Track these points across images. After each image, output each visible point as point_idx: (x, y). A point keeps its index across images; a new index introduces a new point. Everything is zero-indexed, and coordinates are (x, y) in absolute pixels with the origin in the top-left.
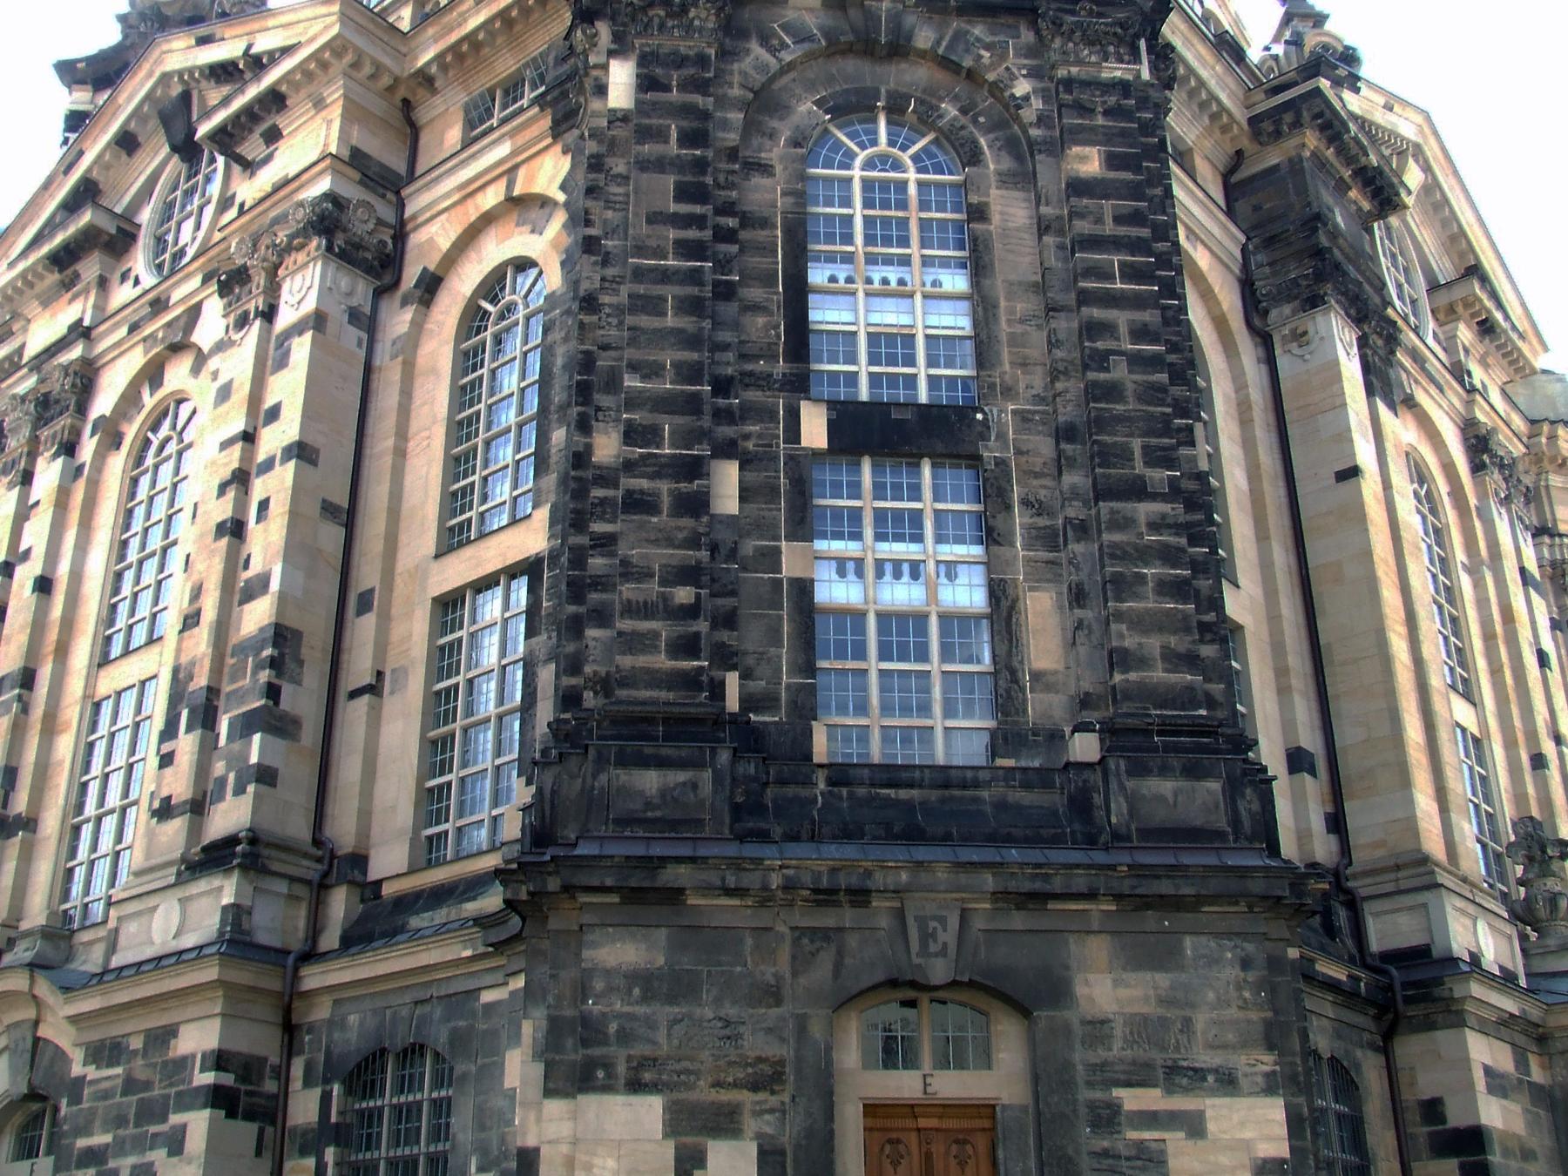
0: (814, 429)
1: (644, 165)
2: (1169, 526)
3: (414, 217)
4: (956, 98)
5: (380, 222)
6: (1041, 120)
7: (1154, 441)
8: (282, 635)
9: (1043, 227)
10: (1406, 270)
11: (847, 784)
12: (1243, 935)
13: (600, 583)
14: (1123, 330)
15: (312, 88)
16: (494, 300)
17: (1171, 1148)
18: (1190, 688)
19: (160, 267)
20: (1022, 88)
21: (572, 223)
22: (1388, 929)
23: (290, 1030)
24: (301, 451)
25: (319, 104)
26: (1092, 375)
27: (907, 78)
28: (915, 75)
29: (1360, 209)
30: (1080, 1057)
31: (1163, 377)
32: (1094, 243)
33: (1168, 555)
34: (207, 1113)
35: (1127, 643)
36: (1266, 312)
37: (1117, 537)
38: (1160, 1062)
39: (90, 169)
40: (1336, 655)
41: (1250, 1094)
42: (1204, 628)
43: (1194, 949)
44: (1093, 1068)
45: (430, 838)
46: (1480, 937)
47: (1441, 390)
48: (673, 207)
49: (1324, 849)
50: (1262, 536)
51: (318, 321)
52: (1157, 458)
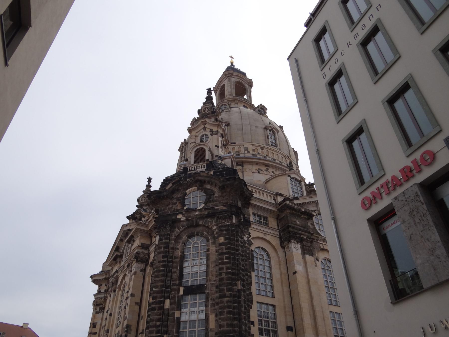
1: (158, 253)
6: (217, 233)
8: (128, 326)
9: (217, 251)
14: (225, 268)
18: (230, 330)
20: (215, 228)
24: (132, 295)
25: (138, 236)
26: (219, 277)
28: (201, 228)
31: (230, 276)
33: (229, 307)
35: (221, 323)
36: (284, 243)
37: (221, 305)
48: (162, 259)
51: (135, 273)
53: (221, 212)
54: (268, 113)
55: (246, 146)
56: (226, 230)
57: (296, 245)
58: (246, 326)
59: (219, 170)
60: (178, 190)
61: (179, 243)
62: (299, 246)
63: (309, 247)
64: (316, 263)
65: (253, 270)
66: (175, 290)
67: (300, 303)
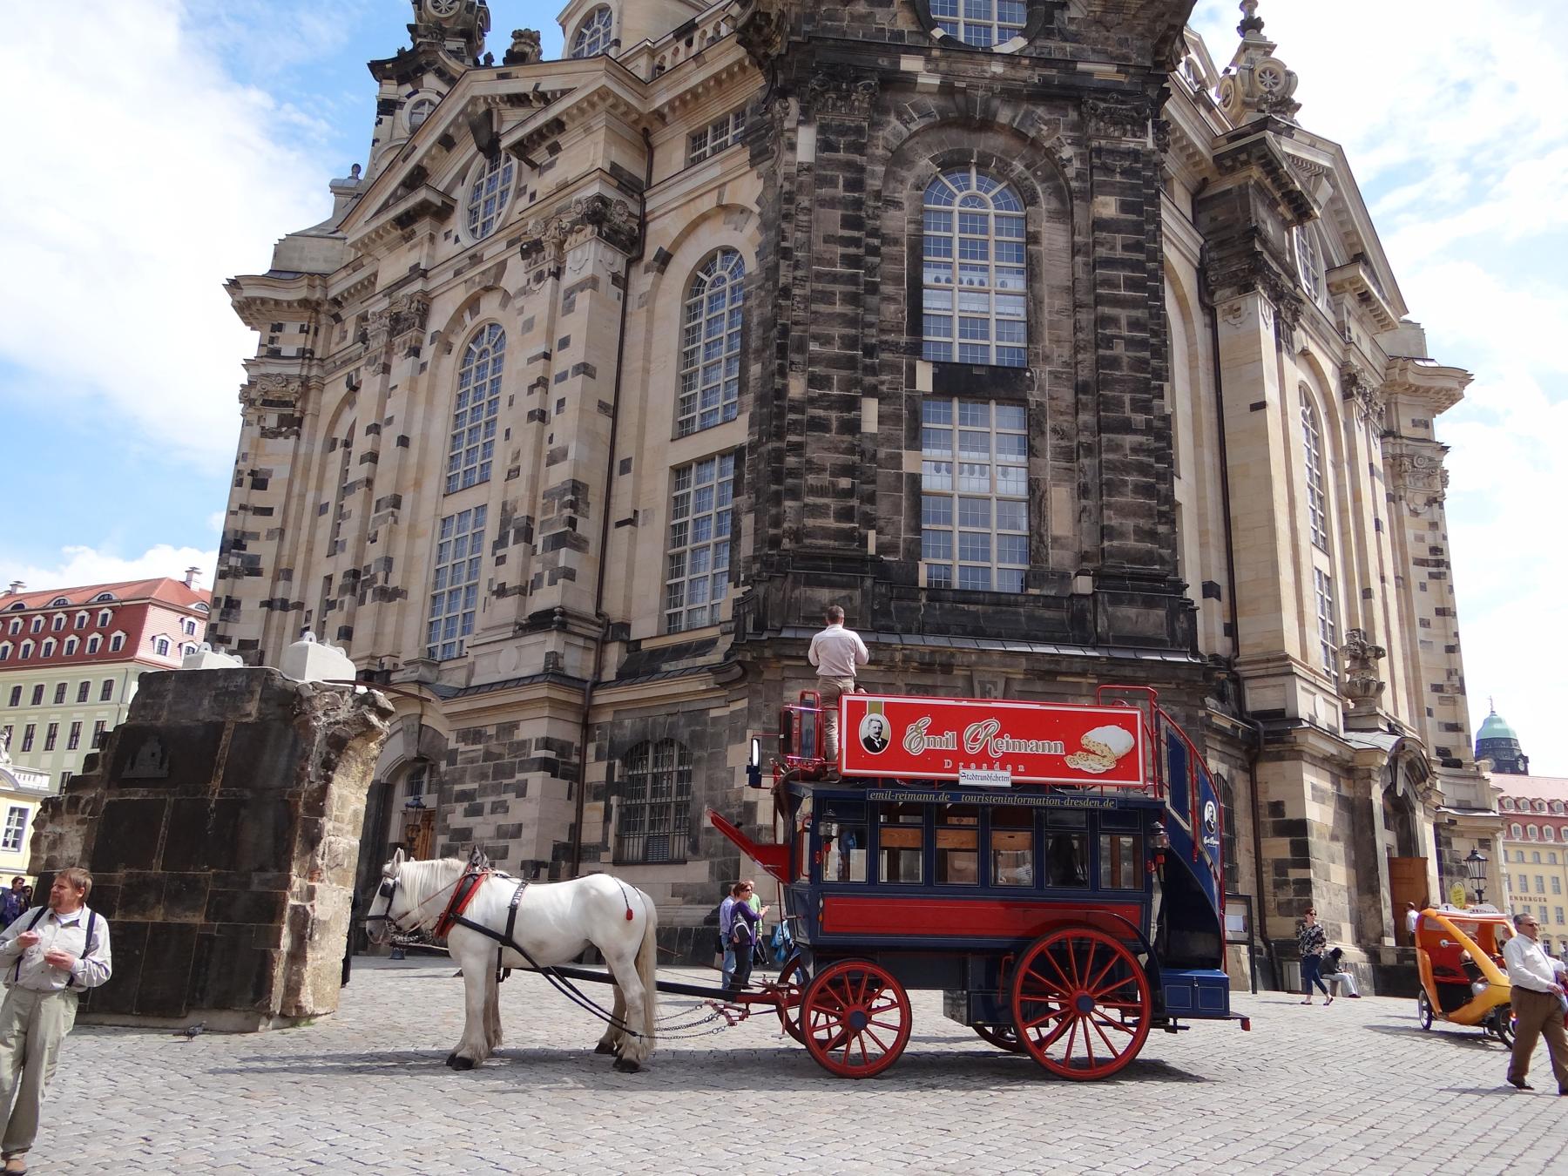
0: (925, 379)
3: (652, 212)
4: (1023, 157)
5: (631, 215)
8: (577, 487)
9: (1075, 250)
10: (1313, 256)
11: (939, 601)
12: (1174, 703)
13: (794, 473)
14: (1124, 322)
15: (582, 120)
16: (708, 273)
18: (1150, 552)
19: (474, 231)
20: (1067, 152)
21: (765, 226)
22: (1259, 698)
23: (587, 728)
24: (585, 369)
25: (588, 130)
26: (1101, 352)
27: (992, 142)
28: (993, 143)
31: (1147, 354)
32: (1109, 263)
33: (1143, 469)
34: (541, 773)
35: (1113, 523)
36: (1212, 294)
37: (1111, 456)
39: (421, 160)
42: (1161, 514)
45: (670, 616)
46: (1317, 707)
49: (1221, 646)
50: (1197, 444)
53: (1104, 90)
66: (895, 368)
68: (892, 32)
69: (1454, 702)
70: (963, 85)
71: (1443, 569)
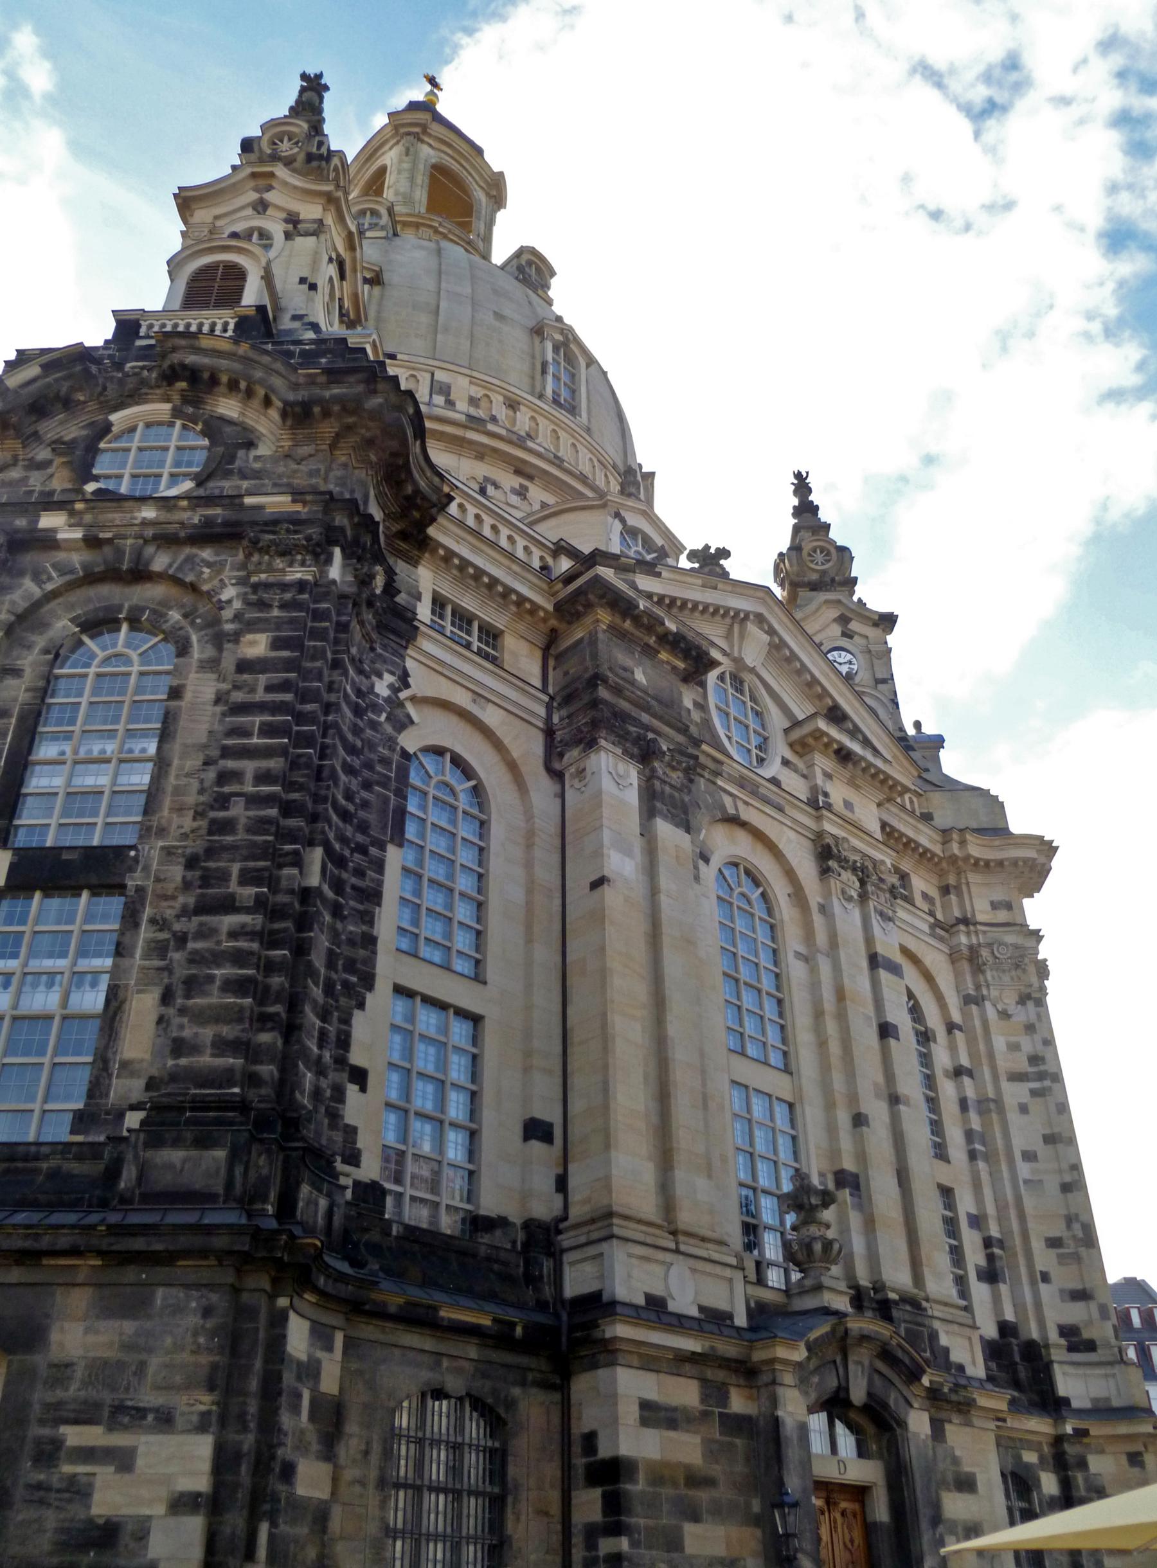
2: (247, 934)
6: (237, 617)
7: (251, 864)
9: (218, 701)
12: (211, 1287)
14: (249, 776)
17: (98, 1482)
18: (230, 1070)
22: (577, 1280)
26: (213, 814)
28: (153, 592)
29: (674, 668)
30: (40, 1396)
31: (273, 812)
33: (239, 957)
35: (187, 1033)
36: (561, 755)
37: (199, 945)
38: (109, 1401)
40: (576, 1036)
41: (183, 1432)
43: (164, 1299)
44: (48, 1407)
47: (780, 809)
52: (246, 879)
53: (273, 523)
54: (557, 289)
55: (440, 376)
56: (283, 606)
57: (622, 767)
58: (321, 1072)
59: (297, 349)
60: (67, 404)
61: (29, 647)
62: (632, 774)
63: (680, 790)
64: (696, 868)
65: (399, 838)
67: (604, 1014)
68: (42, 493)
69: (1077, 1258)
70: (109, 535)
71: (1047, 1083)
